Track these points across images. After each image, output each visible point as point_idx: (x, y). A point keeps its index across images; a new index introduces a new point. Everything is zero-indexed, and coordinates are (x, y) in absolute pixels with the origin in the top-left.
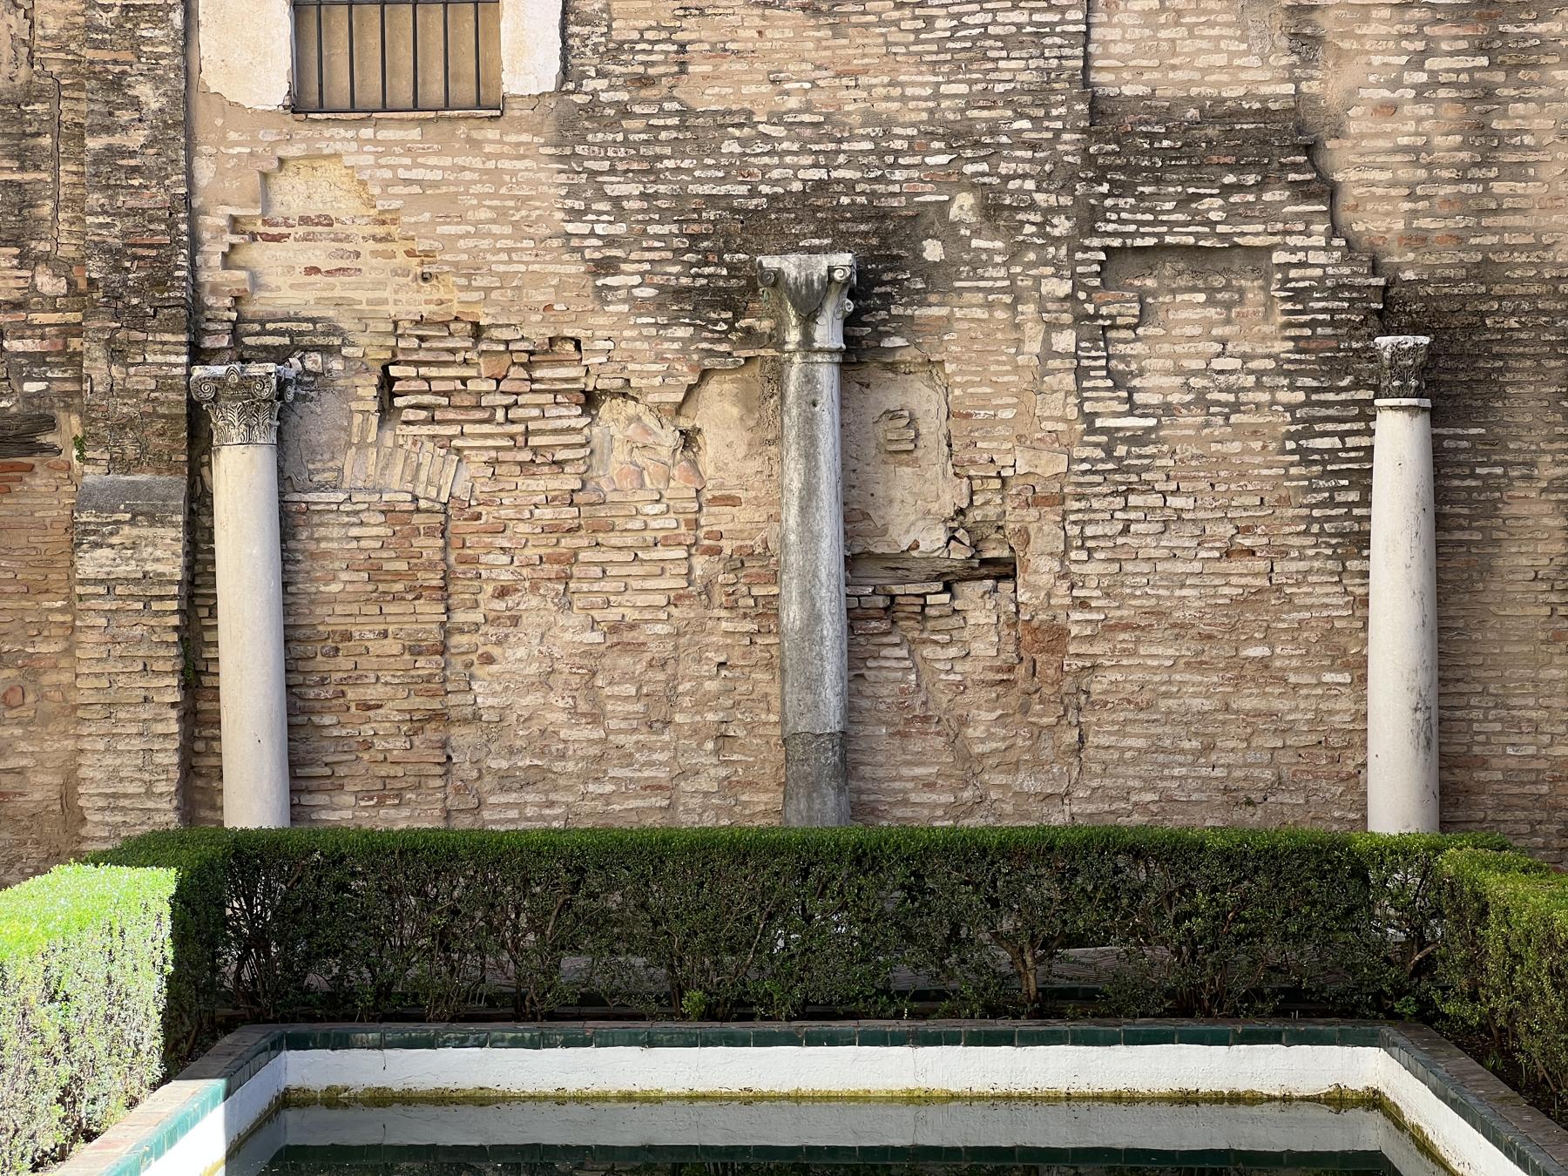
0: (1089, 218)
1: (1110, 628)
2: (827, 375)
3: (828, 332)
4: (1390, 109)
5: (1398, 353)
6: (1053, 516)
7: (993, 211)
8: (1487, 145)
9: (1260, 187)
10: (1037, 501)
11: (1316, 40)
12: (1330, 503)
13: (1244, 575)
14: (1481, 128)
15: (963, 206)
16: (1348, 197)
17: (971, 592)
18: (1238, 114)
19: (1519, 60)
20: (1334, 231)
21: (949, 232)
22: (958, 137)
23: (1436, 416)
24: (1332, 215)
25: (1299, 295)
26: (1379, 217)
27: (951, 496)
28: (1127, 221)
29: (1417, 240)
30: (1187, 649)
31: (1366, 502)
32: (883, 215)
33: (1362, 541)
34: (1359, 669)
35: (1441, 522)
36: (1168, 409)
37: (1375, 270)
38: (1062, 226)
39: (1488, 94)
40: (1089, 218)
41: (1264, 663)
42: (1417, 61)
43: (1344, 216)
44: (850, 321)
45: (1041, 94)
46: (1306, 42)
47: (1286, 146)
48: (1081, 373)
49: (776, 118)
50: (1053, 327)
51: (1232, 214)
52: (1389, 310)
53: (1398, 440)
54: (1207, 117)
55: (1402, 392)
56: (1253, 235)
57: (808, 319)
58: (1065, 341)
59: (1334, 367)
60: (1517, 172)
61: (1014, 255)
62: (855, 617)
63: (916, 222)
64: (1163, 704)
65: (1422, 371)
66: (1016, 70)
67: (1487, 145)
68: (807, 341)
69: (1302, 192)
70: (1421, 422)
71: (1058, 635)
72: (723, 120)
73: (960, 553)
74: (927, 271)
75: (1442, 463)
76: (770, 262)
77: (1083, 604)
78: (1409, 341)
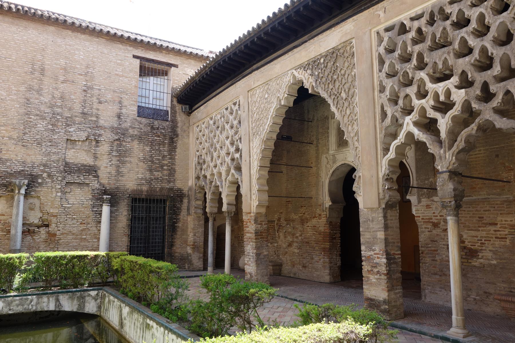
0: (64, 178)
1: (62, 234)
2: (22, 198)
3: (23, 191)
4: (106, 167)
5: (107, 198)
6: (56, 218)
7: (49, 176)
8: (119, 173)
9: (89, 175)
10: (53, 216)
11: (97, 157)
12: (96, 217)
13: (83, 227)
14: (118, 171)
15: (45, 175)
16: (100, 178)
17: (41, 229)
18: (87, 166)
19: (123, 163)
20: (98, 182)
21: (43, 178)
22: (45, 165)
23: (111, 206)
24: (98, 180)
25: (93, 190)
26: (104, 181)
27: (40, 215)
28: (69, 178)
29: (109, 184)
30: (74, 237)
31: (101, 217)
32: (32, 175)
33: (100, 222)
34: (99, 239)
35: (111, 220)
36: (73, 204)
37: (103, 187)
38: (60, 179)
39: (119, 166)
40: (64, 178)
41: (85, 239)
42: (110, 161)
43: (99, 180)
44: (26, 190)
45: (58, 161)
46: (96, 158)
47: (91, 170)
48: (61, 199)
49: (16, 160)
50: (58, 192)
51: (85, 179)
52: (105, 192)
53: (106, 209)
54: (82, 166)
55: (107, 203)
56: (87, 181)
57: (19, 190)
58: (59, 194)
59: (98, 199)
60: (122, 176)
61: (53, 182)
62: (23, 232)
63: (37, 176)
64: (71, 244)
65: (109, 200)
66: (54, 157)
67: (119, 173)
68: (19, 192)
69: (95, 177)
70: (109, 207)
71: (55, 235)
72: (7, 160)
73: (40, 223)
74: (39, 183)
75: (111, 212)
76: (13, 181)
77: (59, 230)
78: (108, 197)
